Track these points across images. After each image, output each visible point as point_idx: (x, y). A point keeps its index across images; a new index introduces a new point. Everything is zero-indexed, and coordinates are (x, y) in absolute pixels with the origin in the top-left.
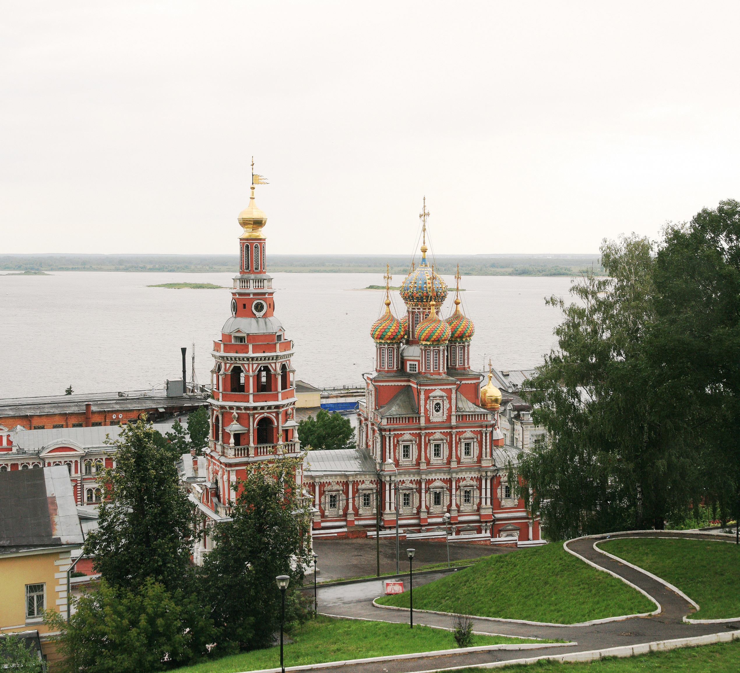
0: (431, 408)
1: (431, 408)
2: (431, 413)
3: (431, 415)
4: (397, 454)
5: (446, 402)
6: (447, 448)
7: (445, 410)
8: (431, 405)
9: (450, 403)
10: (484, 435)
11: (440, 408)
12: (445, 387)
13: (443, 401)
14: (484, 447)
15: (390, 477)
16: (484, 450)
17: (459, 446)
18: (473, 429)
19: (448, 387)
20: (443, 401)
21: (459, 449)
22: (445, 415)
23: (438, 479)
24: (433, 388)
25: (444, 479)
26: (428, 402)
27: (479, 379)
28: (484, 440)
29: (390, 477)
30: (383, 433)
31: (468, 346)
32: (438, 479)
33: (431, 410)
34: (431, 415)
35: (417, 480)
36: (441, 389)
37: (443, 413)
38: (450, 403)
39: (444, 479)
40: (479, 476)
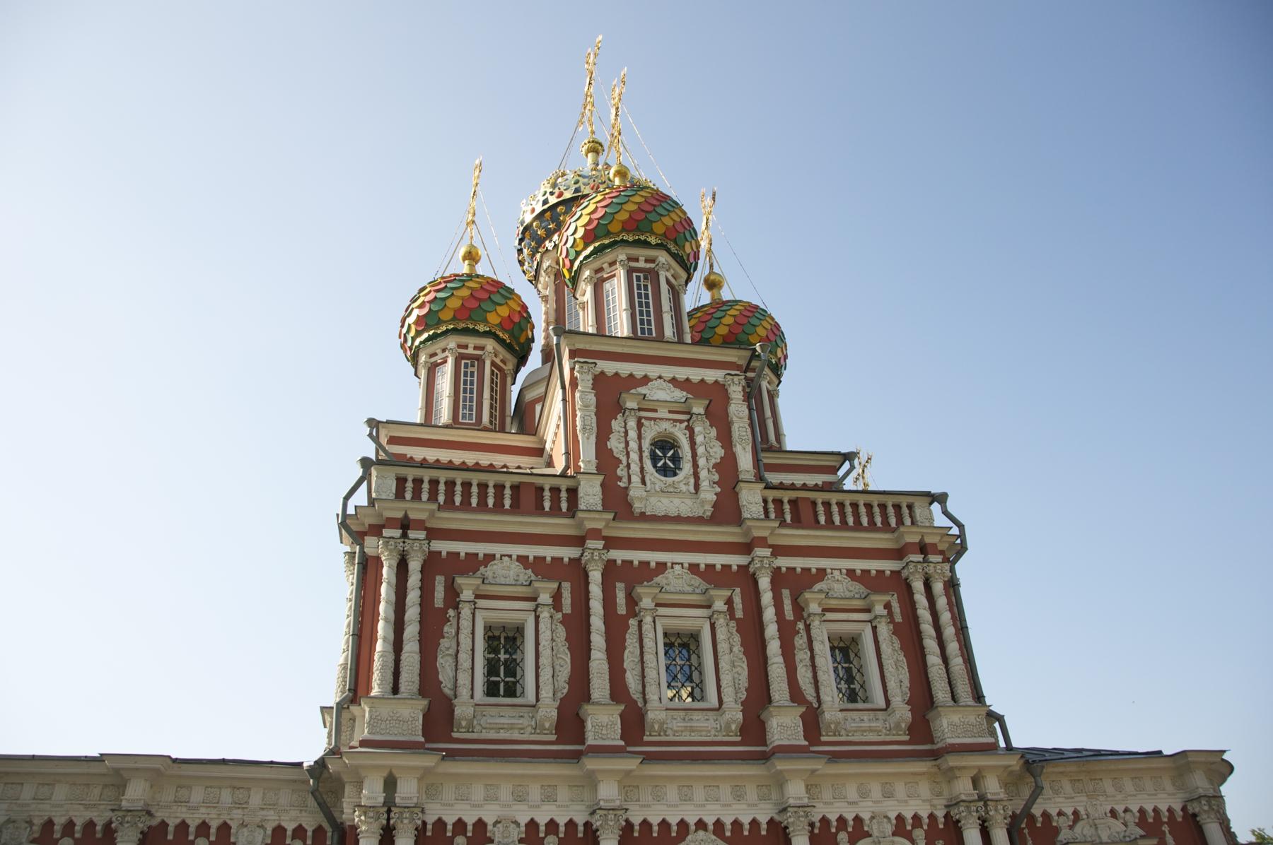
0: (633, 445)
1: (633, 445)
2: (635, 468)
3: (636, 479)
4: (444, 664)
5: (705, 433)
6: (737, 648)
7: (702, 462)
8: (633, 434)
9: (725, 438)
10: (918, 586)
11: (676, 459)
12: (695, 374)
13: (690, 430)
14: (931, 644)
15: (390, 784)
16: (934, 659)
17: (800, 641)
18: (859, 565)
19: (711, 375)
20: (690, 430)
21: (802, 656)
22: (705, 484)
23: (701, 825)
24: (639, 370)
25: (737, 824)
26: (616, 425)
27: (834, 470)
28: (924, 613)
29: (390, 784)
30: (370, 541)
31: (773, 396)
32: (701, 825)
33: (634, 456)
34: (636, 479)
35: (571, 824)
36: (674, 381)
37: (696, 476)
38: (725, 438)
39: (737, 824)
40: (940, 814)
